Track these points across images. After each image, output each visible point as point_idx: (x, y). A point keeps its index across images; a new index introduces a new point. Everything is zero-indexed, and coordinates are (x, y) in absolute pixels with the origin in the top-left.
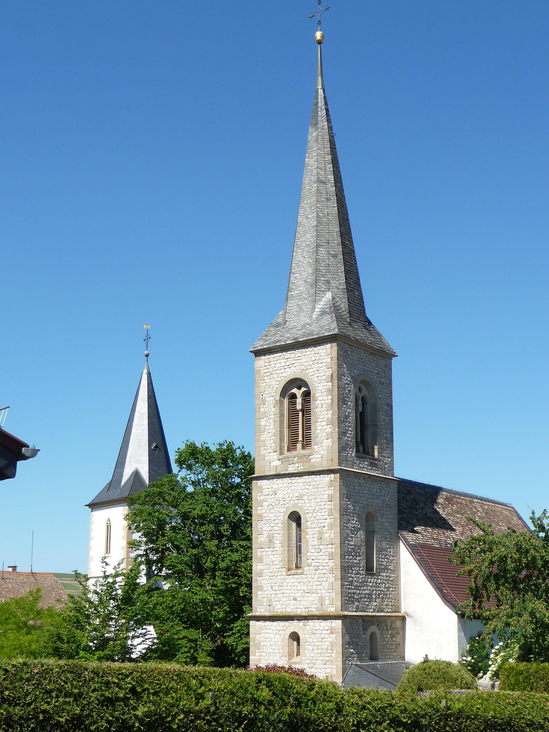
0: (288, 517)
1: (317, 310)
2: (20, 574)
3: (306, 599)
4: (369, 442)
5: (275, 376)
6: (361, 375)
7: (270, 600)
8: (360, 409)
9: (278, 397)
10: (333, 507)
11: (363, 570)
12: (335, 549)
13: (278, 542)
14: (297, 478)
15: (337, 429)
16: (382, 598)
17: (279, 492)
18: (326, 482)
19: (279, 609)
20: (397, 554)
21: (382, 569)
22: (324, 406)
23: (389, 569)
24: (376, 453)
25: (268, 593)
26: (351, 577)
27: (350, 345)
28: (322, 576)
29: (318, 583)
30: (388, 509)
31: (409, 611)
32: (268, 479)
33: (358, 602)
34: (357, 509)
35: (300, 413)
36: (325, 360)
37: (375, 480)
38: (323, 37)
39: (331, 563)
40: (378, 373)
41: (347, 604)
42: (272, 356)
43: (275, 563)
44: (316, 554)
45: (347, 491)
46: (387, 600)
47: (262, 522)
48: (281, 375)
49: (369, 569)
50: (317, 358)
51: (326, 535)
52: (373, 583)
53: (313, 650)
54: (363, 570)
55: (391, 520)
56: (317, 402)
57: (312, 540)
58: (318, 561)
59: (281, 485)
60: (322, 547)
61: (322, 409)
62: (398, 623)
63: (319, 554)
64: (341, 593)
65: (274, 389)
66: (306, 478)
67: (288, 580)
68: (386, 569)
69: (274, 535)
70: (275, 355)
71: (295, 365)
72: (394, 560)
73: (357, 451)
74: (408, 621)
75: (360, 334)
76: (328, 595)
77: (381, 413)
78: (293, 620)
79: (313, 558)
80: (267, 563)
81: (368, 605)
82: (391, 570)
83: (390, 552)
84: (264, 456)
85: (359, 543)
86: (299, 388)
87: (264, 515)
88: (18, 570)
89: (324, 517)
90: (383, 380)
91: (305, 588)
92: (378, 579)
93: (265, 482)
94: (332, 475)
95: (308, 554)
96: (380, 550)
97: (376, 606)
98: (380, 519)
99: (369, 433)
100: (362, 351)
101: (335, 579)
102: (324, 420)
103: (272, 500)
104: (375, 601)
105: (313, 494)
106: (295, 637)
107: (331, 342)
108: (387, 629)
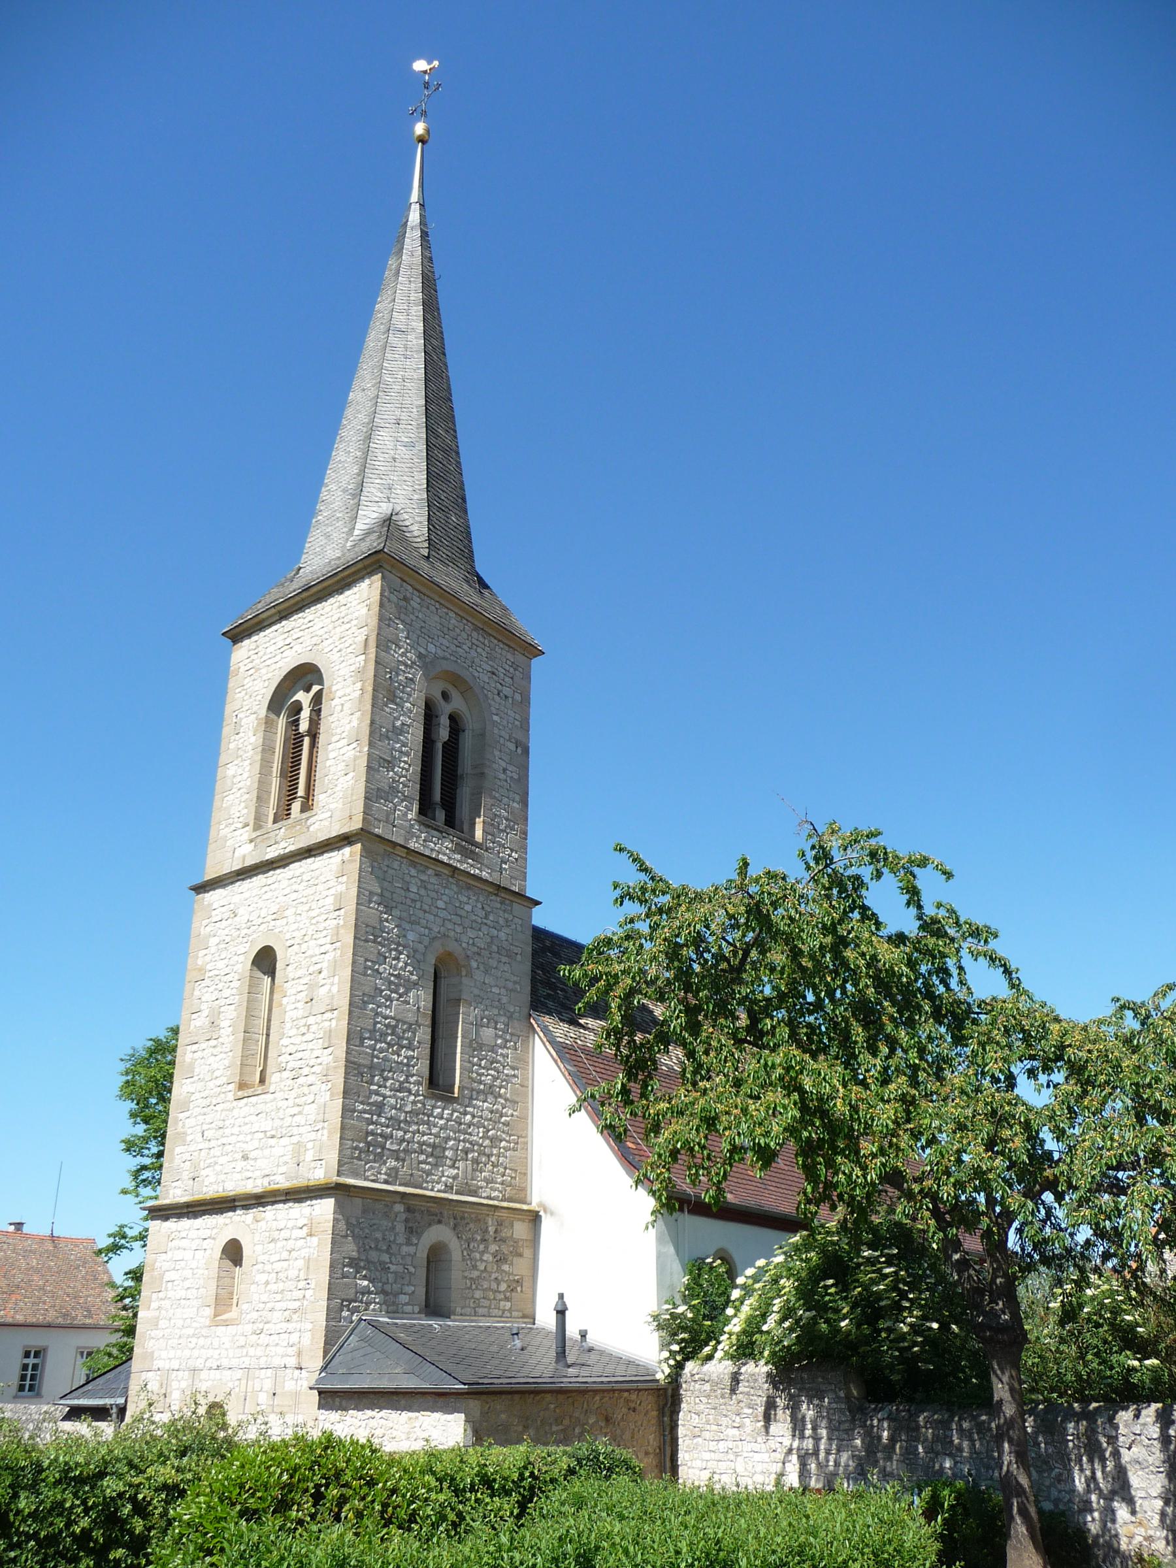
0: (253, 963)
1: (356, 532)
2: (28, 1237)
3: (267, 1152)
4: (463, 810)
5: (264, 671)
6: (444, 658)
7: (196, 1167)
8: (443, 734)
9: (263, 712)
10: (341, 922)
11: (418, 1083)
12: (338, 1020)
13: (228, 1023)
14: (278, 871)
15: (366, 749)
16: (476, 1161)
17: (241, 911)
18: (334, 868)
19: (211, 1189)
20: (523, 1062)
21: (479, 1092)
22: (347, 706)
23: (500, 1096)
24: (479, 834)
25: (192, 1148)
26: (377, 1093)
27: (418, 591)
28: (306, 1090)
29: (296, 1110)
30: (504, 959)
31: (550, 1202)
32: (224, 886)
33: (397, 1159)
34: (411, 936)
35: (307, 740)
36: (356, 614)
37: (469, 887)
38: (428, 131)
39: (326, 1058)
40: (493, 673)
41: (359, 1158)
42: (262, 634)
43: (217, 1073)
44: (298, 1040)
45: (382, 888)
46: (489, 1167)
47: (204, 984)
48: (274, 667)
49: (438, 1081)
50: (342, 615)
51: (323, 991)
52: (448, 1120)
53: (267, 1283)
54: (418, 1083)
55: (510, 985)
56: (333, 703)
57: (293, 1006)
58: (299, 1055)
59: (246, 895)
60: (311, 1020)
61: (341, 715)
62: (520, 1230)
63: (305, 1038)
64: (343, 1128)
65: (259, 697)
66: (296, 868)
67: (236, 1113)
68: (490, 1092)
69: (222, 1009)
70: (268, 631)
71: (300, 640)
72: (514, 1076)
73: (422, 811)
74: (547, 1224)
75: (450, 578)
76: (313, 1136)
77: (497, 753)
78: (233, 1209)
79: (292, 1049)
80: (201, 1076)
81: (429, 1173)
82: (506, 1100)
83: (505, 1056)
84: (225, 839)
85: (411, 1017)
86: (308, 690)
87: (209, 967)
88: (25, 1229)
89: (323, 950)
90: (507, 691)
91: (267, 1125)
92: (465, 1113)
93: (220, 892)
94: (347, 851)
95: (282, 1042)
96: (475, 1046)
97: (455, 1178)
98: (478, 976)
99: (465, 793)
100: (452, 614)
101: (332, 1095)
102: (344, 735)
103: (226, 932)
104: (453, 1166)
105: (304, 900)
106: (233, 1252)
107: (371, 574)
108: (484, 1240)
